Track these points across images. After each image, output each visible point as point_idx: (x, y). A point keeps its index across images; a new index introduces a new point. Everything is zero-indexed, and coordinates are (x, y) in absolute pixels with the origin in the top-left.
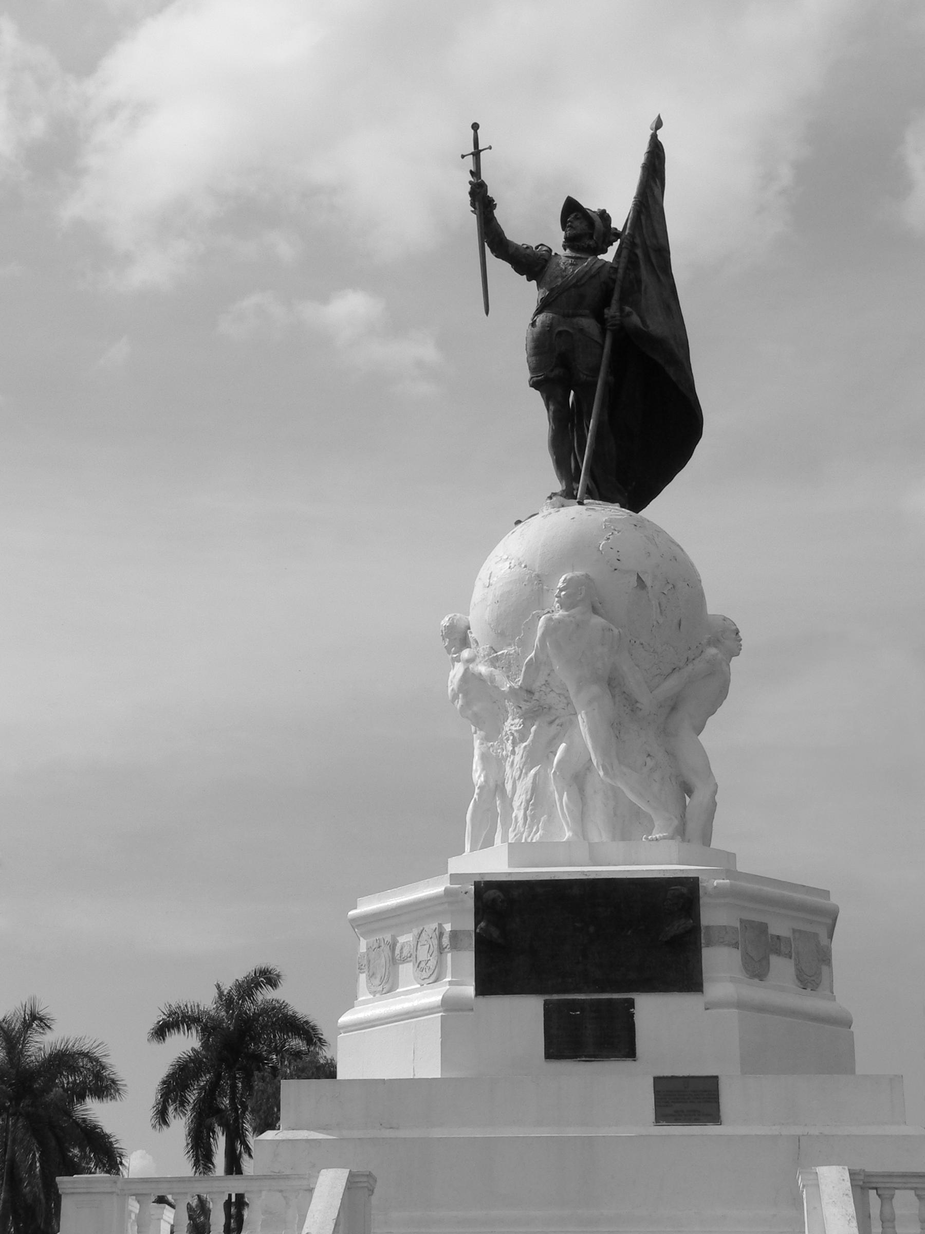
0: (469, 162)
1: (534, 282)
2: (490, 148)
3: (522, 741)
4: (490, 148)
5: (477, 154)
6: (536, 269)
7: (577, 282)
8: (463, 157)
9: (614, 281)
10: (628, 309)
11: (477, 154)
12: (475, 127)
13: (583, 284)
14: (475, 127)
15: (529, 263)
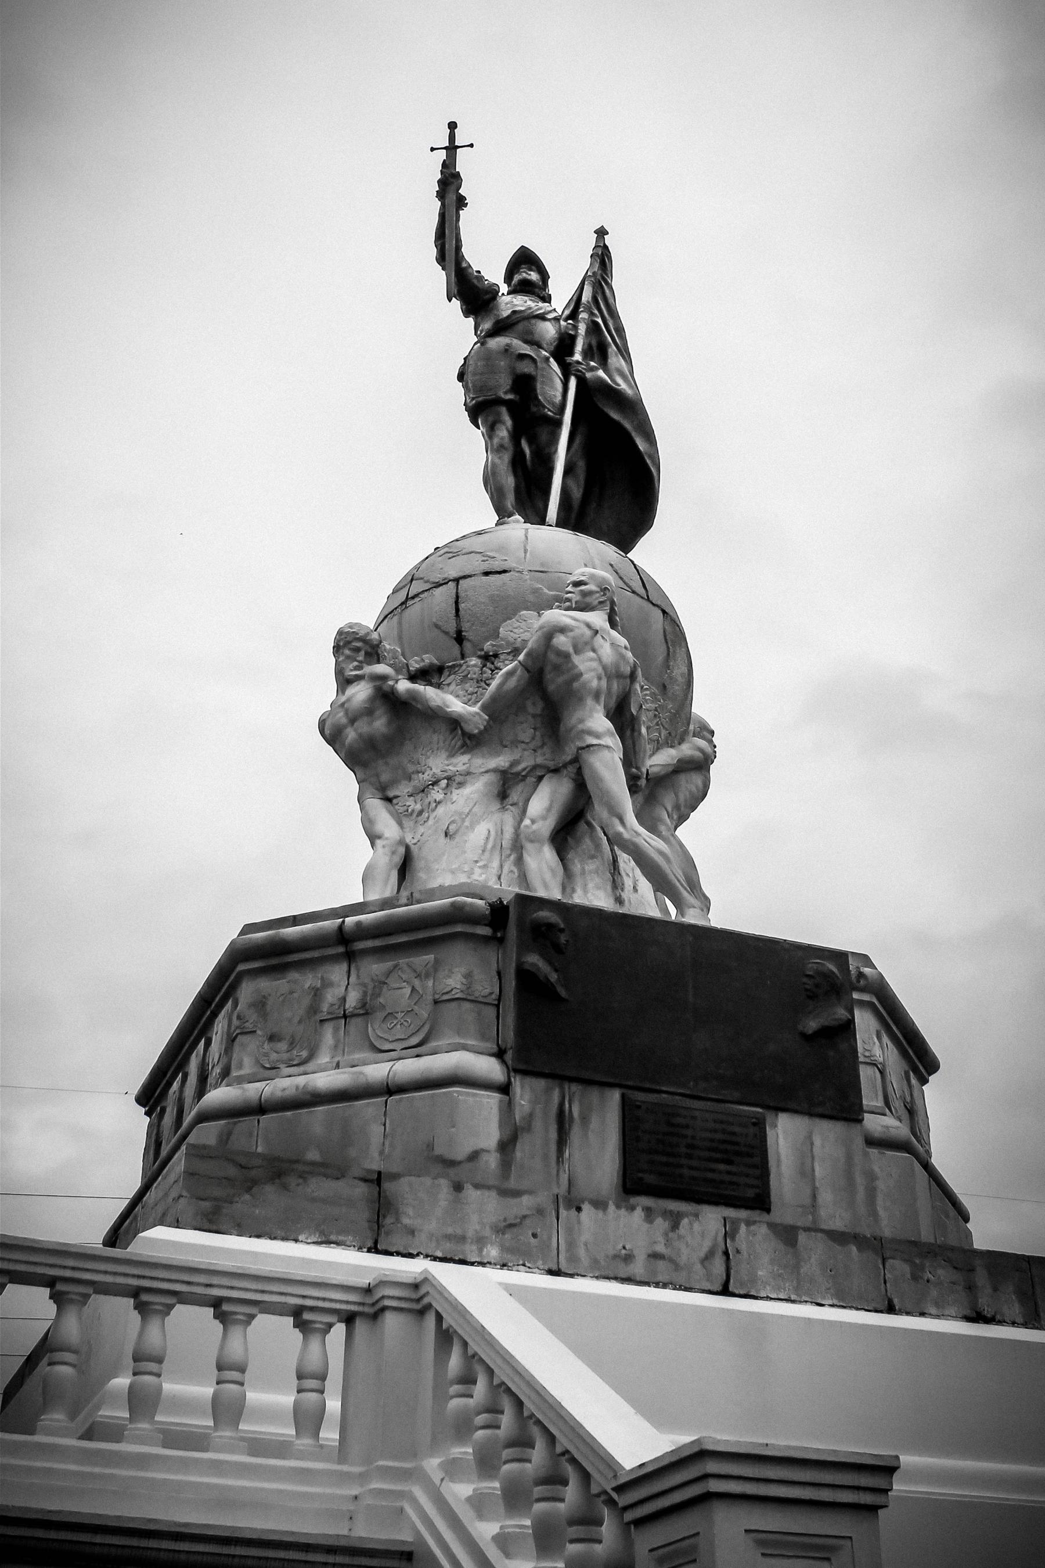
0: (442, 155)
1: (471, 321)
2: (471, 146)
3: (461, 785)
4: (471, 146)
5: (452, 149)
6: (487, 296)
7: (544, 313)
8: (432, 149)
9: (573, 339)
10: (592, 363)
11: (452, 149)
12: (453, 126)
13: (549, 320)
14: (453, 126)
15: (471, 293)
